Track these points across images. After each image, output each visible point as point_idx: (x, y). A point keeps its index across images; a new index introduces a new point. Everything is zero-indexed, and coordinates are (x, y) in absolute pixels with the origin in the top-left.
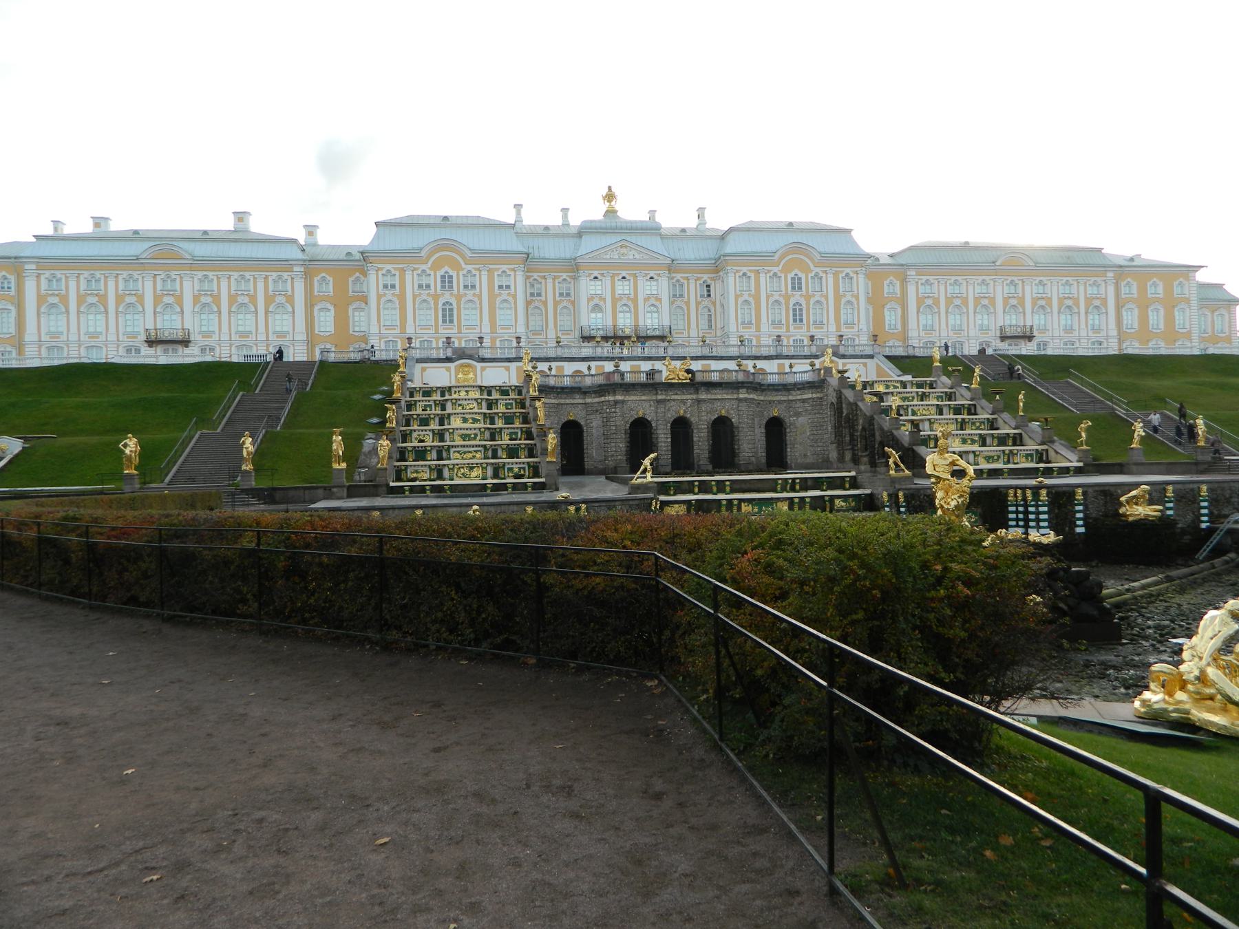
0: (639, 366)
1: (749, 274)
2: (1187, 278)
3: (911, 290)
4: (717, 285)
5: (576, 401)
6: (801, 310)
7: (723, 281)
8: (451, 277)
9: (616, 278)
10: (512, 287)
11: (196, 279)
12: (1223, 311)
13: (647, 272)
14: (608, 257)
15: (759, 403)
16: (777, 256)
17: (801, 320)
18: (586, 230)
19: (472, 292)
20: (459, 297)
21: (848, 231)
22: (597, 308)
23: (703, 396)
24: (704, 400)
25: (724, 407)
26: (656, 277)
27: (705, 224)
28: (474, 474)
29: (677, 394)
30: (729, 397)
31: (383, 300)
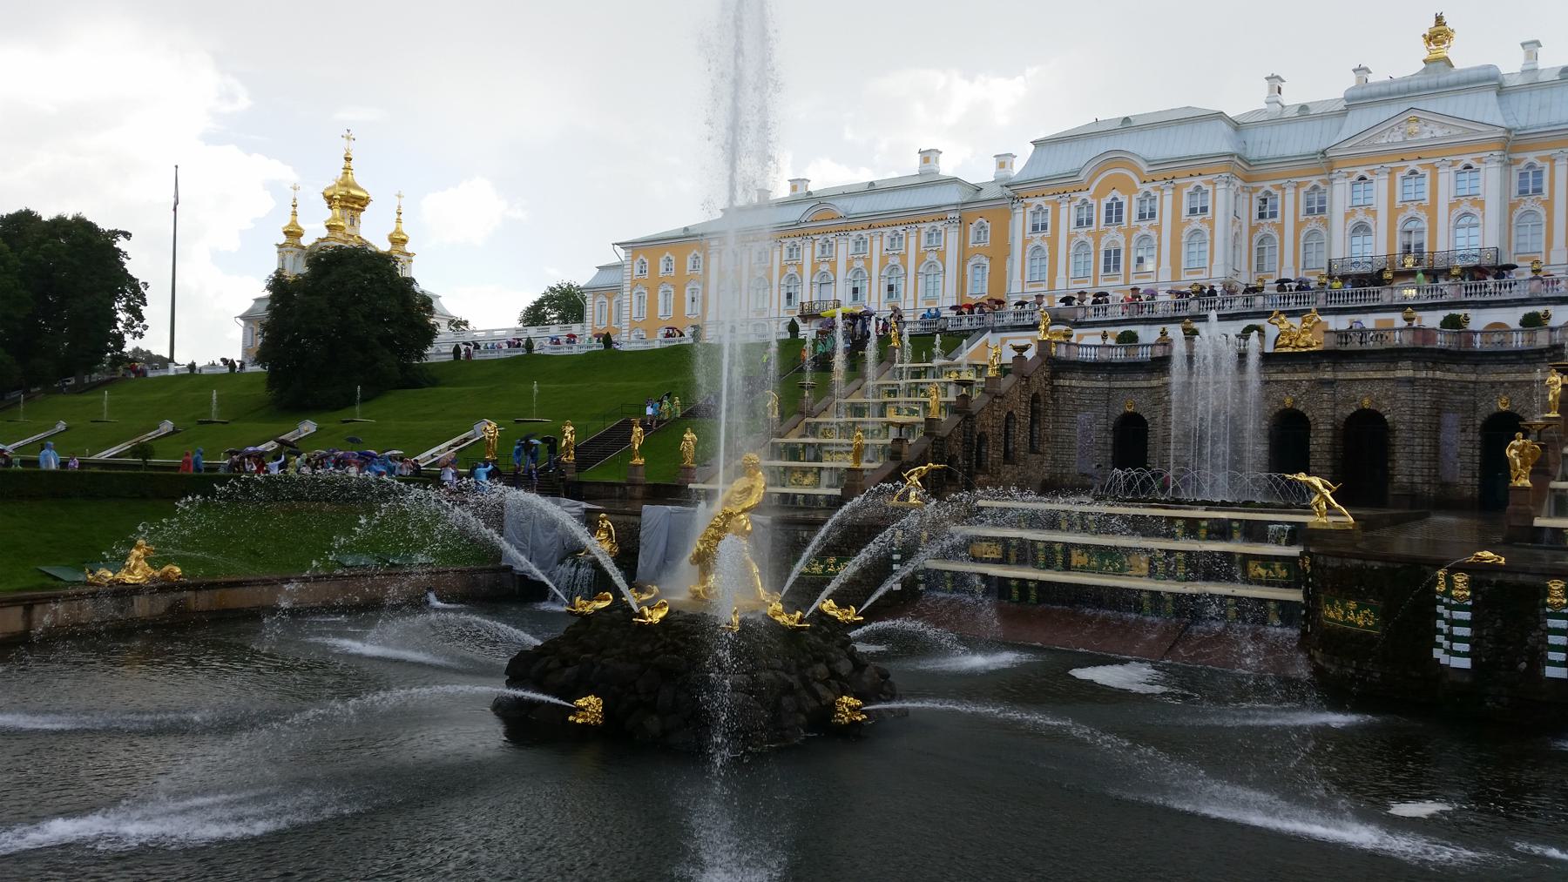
0: (1327, 323)
5: (1137, 384)
8: (1120, 205)
9: (1398, 176)
11: (850, 241)
13: (1454, 158)
14: (1384, 141)
15: (1464, 386)
18: (1356, 101)
19: (1148, 223)
22: (1361, 229)
24: (1331, 383)
25: (1370, 395)
26: (1475, 165)
28: (806, 481)
29: (1283, 372)
30: (1379, 375)
31: (1029, 247)
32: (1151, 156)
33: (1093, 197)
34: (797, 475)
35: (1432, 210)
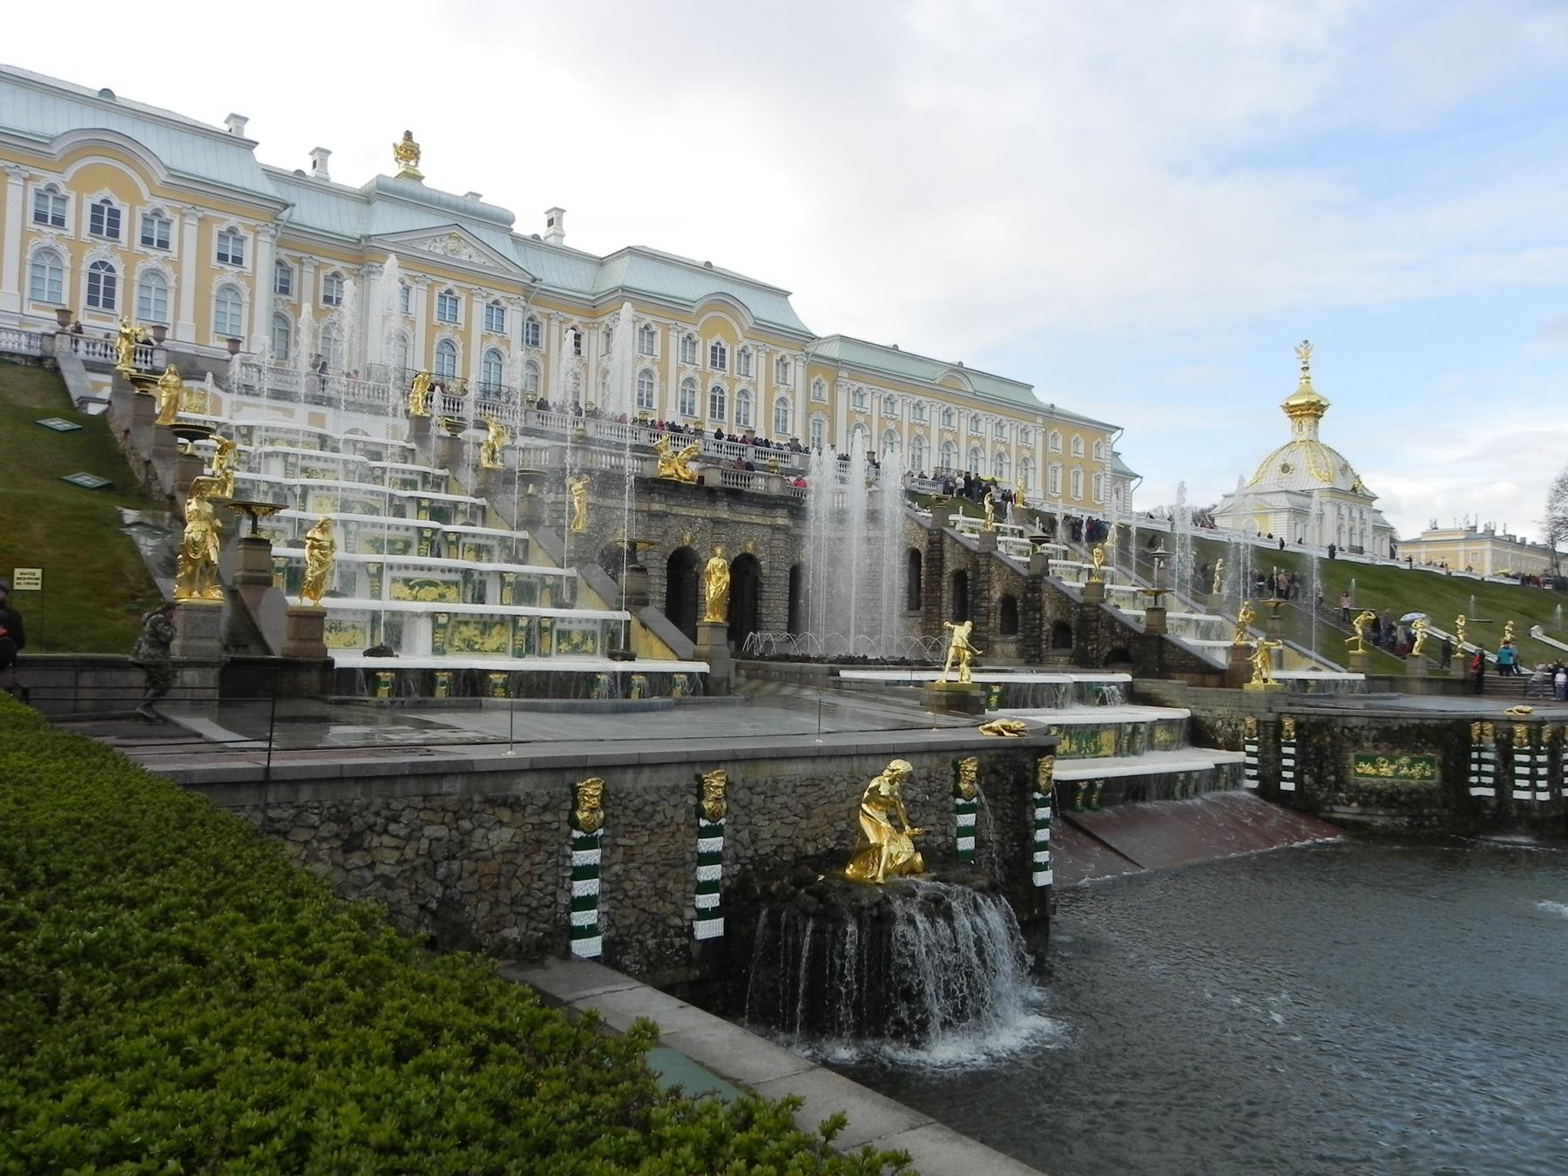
1: (654, 328)
2: (1104, 442)
3: (842, 398)
4: (594, 338)
6: (722, 400)
7: (608, 335)
8: (115, 213)
10: (247, 261)
12: (1119, 485)
14: (425, 248)
16: (698, 306)
17: (721, 416)
19: (161, 254)
20: (130, 258)
21: (786, 294)
23: (723, 512)
25: (750, 539)
26: (503, 303)
27: (563, 236)
30: (759, 520)
32: (177, 164)
33: (68, 185)
34: (469, 632)
35: (466, 335)
